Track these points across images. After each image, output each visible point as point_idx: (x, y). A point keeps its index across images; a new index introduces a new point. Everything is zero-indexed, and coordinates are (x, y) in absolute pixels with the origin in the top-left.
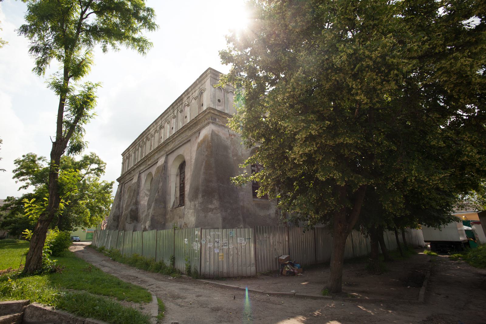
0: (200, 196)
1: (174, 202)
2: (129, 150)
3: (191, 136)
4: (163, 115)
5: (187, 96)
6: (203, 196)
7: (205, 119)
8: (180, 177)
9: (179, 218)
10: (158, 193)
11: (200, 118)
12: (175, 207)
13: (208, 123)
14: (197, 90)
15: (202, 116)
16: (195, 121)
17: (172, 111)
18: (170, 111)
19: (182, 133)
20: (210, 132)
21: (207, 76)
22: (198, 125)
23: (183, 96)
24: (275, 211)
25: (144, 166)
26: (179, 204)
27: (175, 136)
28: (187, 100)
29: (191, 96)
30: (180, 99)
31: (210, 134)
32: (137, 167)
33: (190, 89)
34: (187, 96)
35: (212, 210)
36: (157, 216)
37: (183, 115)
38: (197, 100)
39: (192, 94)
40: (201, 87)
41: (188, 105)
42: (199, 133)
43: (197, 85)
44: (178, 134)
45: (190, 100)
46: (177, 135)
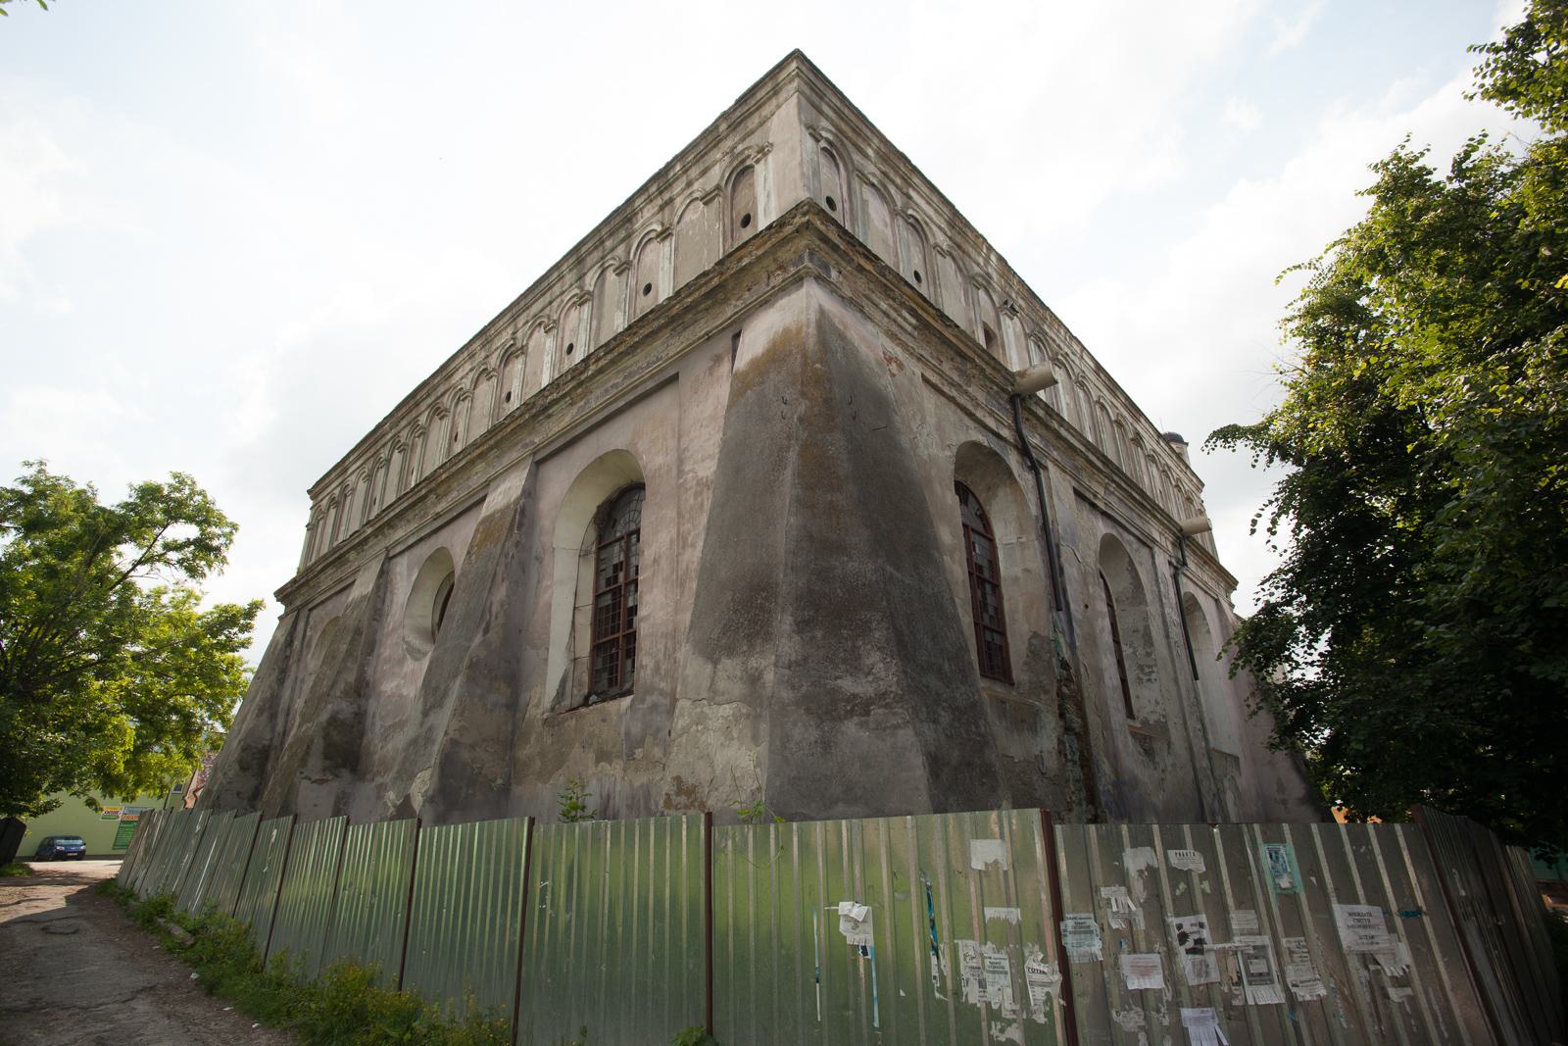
0: (784, 622)
1: (563, 682)
2: (346, 470)
3: (684, 356)
4: (522, 304)
5: (659, 201)
6: (802, 626)
7: (773, 267)
8: (599, 561)
9: (598, 761)
10: (486, 631)
11: (745, 261)
12: (567, 703)
13: (798, 280)
15: (760, 252)
16: (716, 281)
17: (570, 278)
18: (561, 278)
19: (634, 348)
20: (813, 317)
21: (776, 92)
22: (725, 301)
23: (638, 202)
24: (1055, 741)
25: (413, 526)
26: (586, 691)
27: (593, 368)
28: (659, 216)
29: (679, 195)
30: (619, 219)
31: (813, 325)
32: (374, 534)
33: (678, 167)
34: (659, 201)
35: (861, 707)
36: (473, 747)
37: (632, 282)
38: (715, 204)
39: (689, 184)
40: (740, 147)
41: (665, 234)
42: (737, 336)
44: (609, 357)
45: (672, 213)
46: (601, 363)
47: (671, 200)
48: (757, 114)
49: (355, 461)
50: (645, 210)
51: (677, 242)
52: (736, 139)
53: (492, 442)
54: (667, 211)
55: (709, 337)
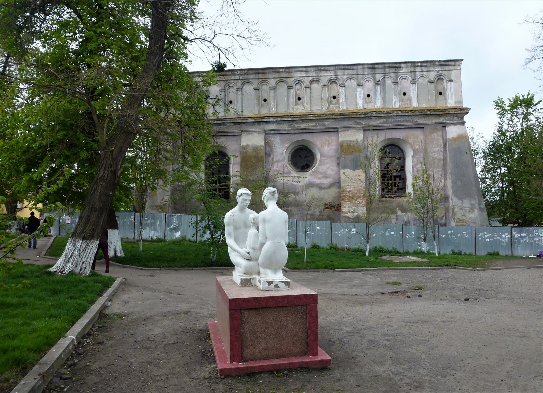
16: (442, 113)
23: (402, 65)
33: (419, 64)
39: (422, 71)
40: (440, 72)
43: (434, 66)
47: (415, 72)
48: (447, 67)
50: (404, 69)
52: (440, 69)
53: (343, 117)
54: (413, 73)
55: (436, 123)
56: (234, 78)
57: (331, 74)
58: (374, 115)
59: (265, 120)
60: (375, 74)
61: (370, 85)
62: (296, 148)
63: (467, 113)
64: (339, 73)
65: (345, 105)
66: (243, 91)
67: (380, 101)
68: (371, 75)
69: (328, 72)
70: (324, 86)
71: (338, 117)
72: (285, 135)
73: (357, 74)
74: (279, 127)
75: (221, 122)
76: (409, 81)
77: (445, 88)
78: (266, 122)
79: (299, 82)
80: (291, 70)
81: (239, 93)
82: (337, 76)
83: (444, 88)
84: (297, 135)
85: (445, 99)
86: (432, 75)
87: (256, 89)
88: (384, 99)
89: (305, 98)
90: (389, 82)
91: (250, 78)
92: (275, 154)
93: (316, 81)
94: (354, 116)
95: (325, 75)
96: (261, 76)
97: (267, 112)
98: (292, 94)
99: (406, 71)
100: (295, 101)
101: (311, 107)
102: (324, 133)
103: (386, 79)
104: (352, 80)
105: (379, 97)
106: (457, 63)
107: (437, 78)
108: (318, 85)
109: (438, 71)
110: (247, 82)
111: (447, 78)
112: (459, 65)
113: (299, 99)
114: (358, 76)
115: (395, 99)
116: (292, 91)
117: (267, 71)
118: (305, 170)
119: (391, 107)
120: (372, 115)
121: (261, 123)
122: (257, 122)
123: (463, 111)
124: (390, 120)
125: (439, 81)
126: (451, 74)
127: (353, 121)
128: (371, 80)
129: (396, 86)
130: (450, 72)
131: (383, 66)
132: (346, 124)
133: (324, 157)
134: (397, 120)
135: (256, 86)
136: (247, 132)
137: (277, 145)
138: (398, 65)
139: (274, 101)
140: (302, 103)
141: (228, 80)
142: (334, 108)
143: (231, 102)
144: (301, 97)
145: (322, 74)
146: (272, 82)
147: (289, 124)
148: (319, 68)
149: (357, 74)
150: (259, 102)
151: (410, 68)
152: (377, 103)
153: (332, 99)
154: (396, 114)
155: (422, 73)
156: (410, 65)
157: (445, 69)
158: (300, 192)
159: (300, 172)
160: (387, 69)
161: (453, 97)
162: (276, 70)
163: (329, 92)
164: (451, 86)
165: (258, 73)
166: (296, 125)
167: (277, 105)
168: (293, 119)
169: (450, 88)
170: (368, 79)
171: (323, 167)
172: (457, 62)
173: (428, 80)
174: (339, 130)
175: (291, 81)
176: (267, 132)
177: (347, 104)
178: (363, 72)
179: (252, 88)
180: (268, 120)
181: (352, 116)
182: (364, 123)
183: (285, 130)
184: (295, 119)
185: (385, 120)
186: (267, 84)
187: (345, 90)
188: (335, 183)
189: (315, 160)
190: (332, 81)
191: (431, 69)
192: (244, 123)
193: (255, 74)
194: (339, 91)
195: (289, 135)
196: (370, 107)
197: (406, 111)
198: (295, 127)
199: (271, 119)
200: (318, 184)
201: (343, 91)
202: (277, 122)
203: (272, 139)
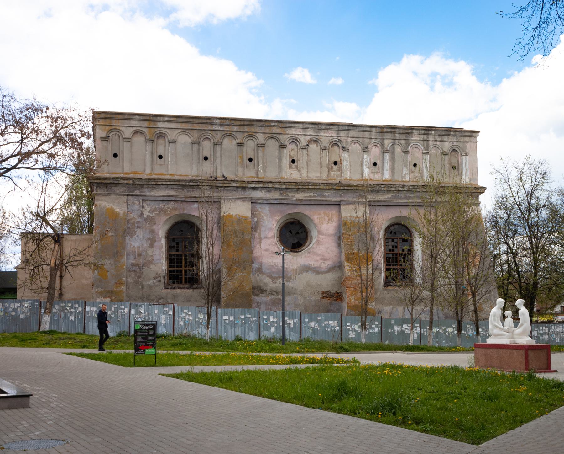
14: (447, 141)
23: (415, 131)
28: (422, 142)
33: (433, 132)
39: (436, 141)
40: (455, 143)
43: (449, 135)
47: (429, 140)
49: (169, 122)
50: (416, 135)
51: (430, 157)
52: (455, 140)
54: (425, 142)
56: (211, 128)
57: (333, 134)
58: (382, 189)
59: (253, 185)
60: (384, 139)
61: (376, 151)
62: (287, 221)
63: (483, 193)
64: (343, 134)
65: (348, 173)
66: (223, 146)
67: (388, 171)
68: (379, 140)
69: (330, 132)
70: (325, 149)
71: (342, 188)
72: (276, 206)
73: (363, 138)
74: (268, 195)
75: (195, 184)
76: (421, 151)
77: (460, 162)
78: (253, 188)
79: (295, 141)
80: (285, 125)
81: (218, 147)
82: (339, 138)
83: (458, 161)
84: (290, 206)
85: (460, 175)
86: (447, 146)
87: (240, 145)
88: (393, 170)
89: (301, 161)
90: (398, 149)
91: (233, 130)
92: (263, 229)
93: (316, 141)
94: (361, 188)
95: (325, 135)
96: (246, 129)
97: (254, 175)
98: (285, 155)
99: (418, 139)
100: (288, 164)
101: (307, 172)
102: (323, 206)
103: (396, 146)
104: (356, 144)
105: (387, 167)
106: (474, 134)
107: (451, 150)
108: (317, 146)
109: (453, 142)
110: (229, 134)
111: (461, 151)
112: (476, 137)
113: (293, 161)
114: (364, 139)
115: (405, 171)
116: (285, 151)
117: (255, 123)
118: (296, 250)
119: (400, 179)
120: (380, 189)
121: (247, 189)
122: (242, 187)
123: (479, 191)
124: (399, 195)
125: (453, 153)
126: (466, 147)
127: (357, 194)
128: (378, 145)
129: (406, 155)
130: (466, 144)
131: (393, 130)
132: (349, 197)
133: (322, 235)
134: (407, 195)
135: (239, 141)
136: (229, 199)
137: (265, 218)
138: (410, 131)
139: (263, 162)
140: (297, 167)
141: (205, 130)
142: (335, 176)
143: (206, 158)
144: (295, 159)
145: (322, 134)
146: (261, 138)
147: (282, 192)
148: (320, 126)
149: (363, 138)
150: (243, 161)
151: (422, 136)
152: (385, 174)
153: (333, 165)
154: (406, 189)
155: (435, 143)
156: (423, 132)
157: (460, 140)
158: (292, 277)
159: (291, 251)
160: (397, 135)
161: (468, 173)
162: (267, 124)
163: (330, 156)
164: (466, 160)
165: (244, 125)
166: (290, 195)
167: (266, 167)
168: (288, 187)
169: (465, 161)
170: (375, 144)
171: (321, 247)
172: (474, 134)
173: (442, 151)
174: (342, 203)
175: (284, 139)
176: (253, 201)
177: (350, 173)
178: (370, 135)
179: (234, 142)
180: (257, 186)
181: (358, 188)
182: (370, 197)
183: (276, 199)
184: (290, 187)
185: (394, 195)
186: (254, 139)
187: (349, 156)
188: (335, 267)
189: (309, 237)
190: (334, 143)
191: (446, 138)
192: (225, 187)
193: (240, 125)
194: (342, 155)
195: (281, 205)
196: (377, 178)
197: (418, 186)
198: (288, 196)
199: (261, 185)
200: (314, 268)
201: (347, 156)
202: (268, 189)
203: (260, 210)
